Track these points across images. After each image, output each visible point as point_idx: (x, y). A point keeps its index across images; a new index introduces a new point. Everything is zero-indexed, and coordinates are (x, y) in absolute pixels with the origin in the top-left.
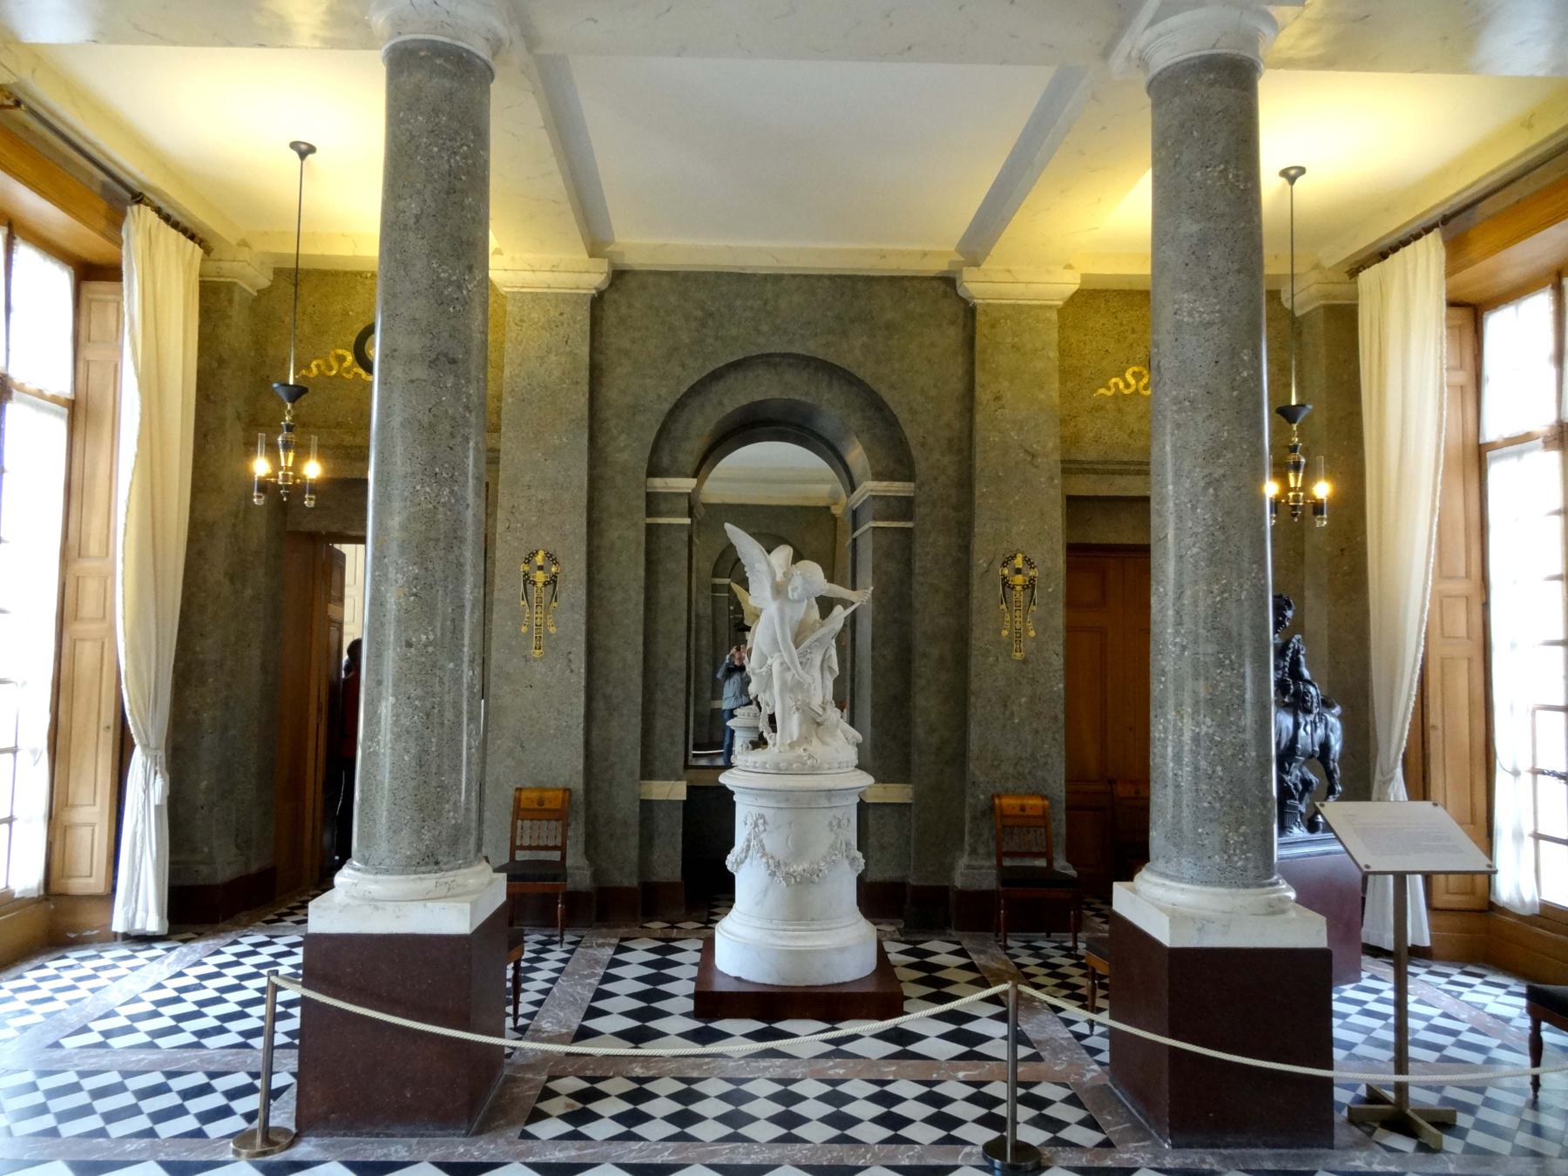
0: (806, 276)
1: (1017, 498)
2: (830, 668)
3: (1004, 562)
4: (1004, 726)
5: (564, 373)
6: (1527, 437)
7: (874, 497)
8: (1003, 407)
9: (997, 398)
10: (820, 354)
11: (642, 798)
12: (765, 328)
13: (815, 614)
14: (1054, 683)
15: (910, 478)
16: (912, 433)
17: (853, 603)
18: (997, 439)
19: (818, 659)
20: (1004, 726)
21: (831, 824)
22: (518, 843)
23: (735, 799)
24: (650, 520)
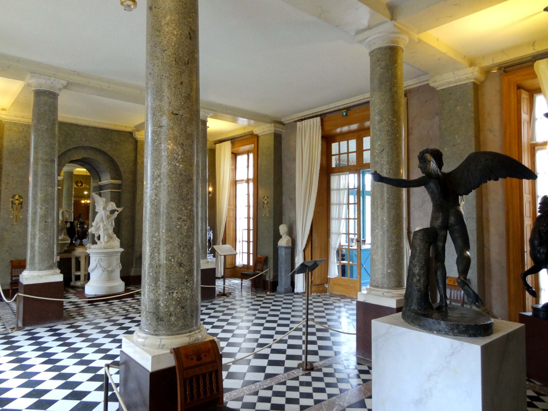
0: (95, 128)
2: (113, 226)
5: (24, 146)
6: (243, 180)
7: (111, 184)
10: (99, 147)
12: (83, 139)
15: (120, 180)
16: (122, 169)
19: (110, 223)
22: (13, 275)
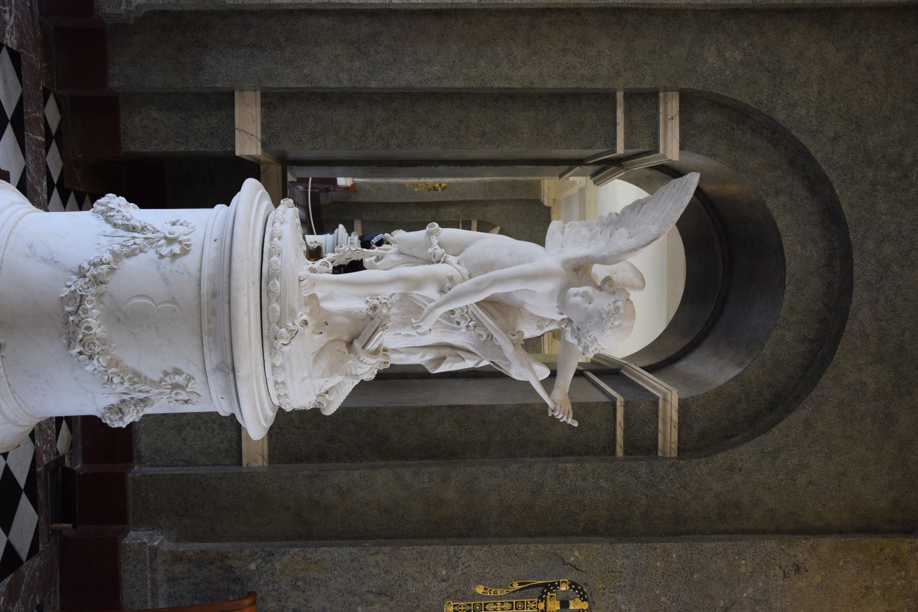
1: (663, 599)
2: (441, 360)
3: (577, 585)
8: (785, 576)
9: (798, 569)
10: (852, 326)
11: (237, 94)
12: (888, 249)
13: (530, 332)
15: (682, 449)
17: (549, 392)
18: (743, 569)
19: (457, 339)
21: (177, 372)
23: (218, 207)
24: (620, 95)
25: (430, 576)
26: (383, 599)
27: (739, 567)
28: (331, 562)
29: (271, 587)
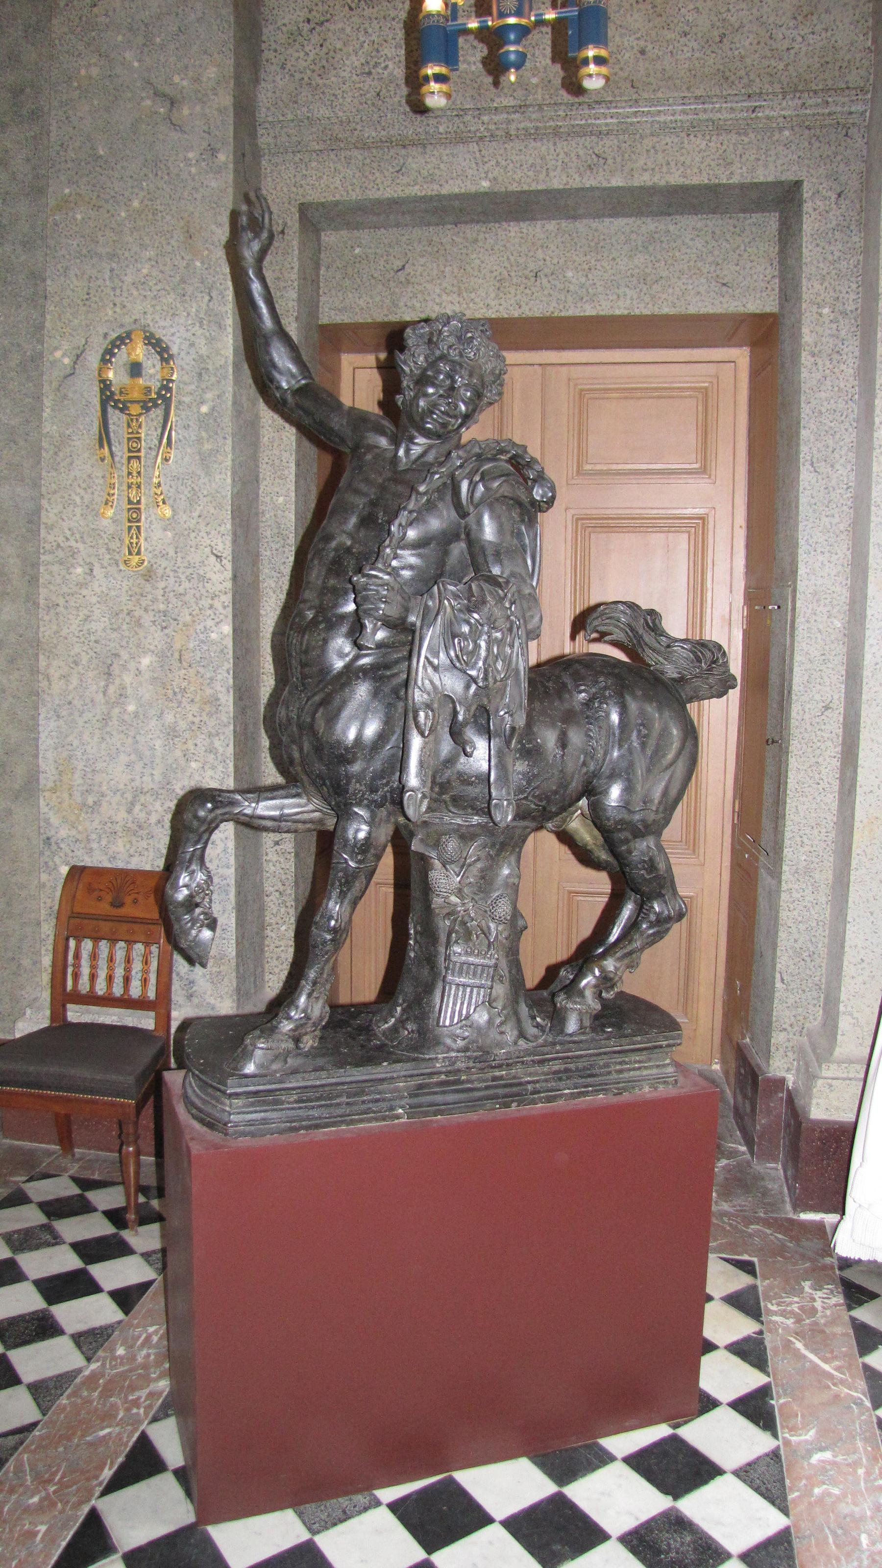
1: (136, 204)
4: (106, 719)
14: (209, 623)
18: (95, 72)
20: (106, 719)
25: (84, 592)
26: (116, 670)
27: (90, 78)
28: (60, 750)
29: (95, 845)
